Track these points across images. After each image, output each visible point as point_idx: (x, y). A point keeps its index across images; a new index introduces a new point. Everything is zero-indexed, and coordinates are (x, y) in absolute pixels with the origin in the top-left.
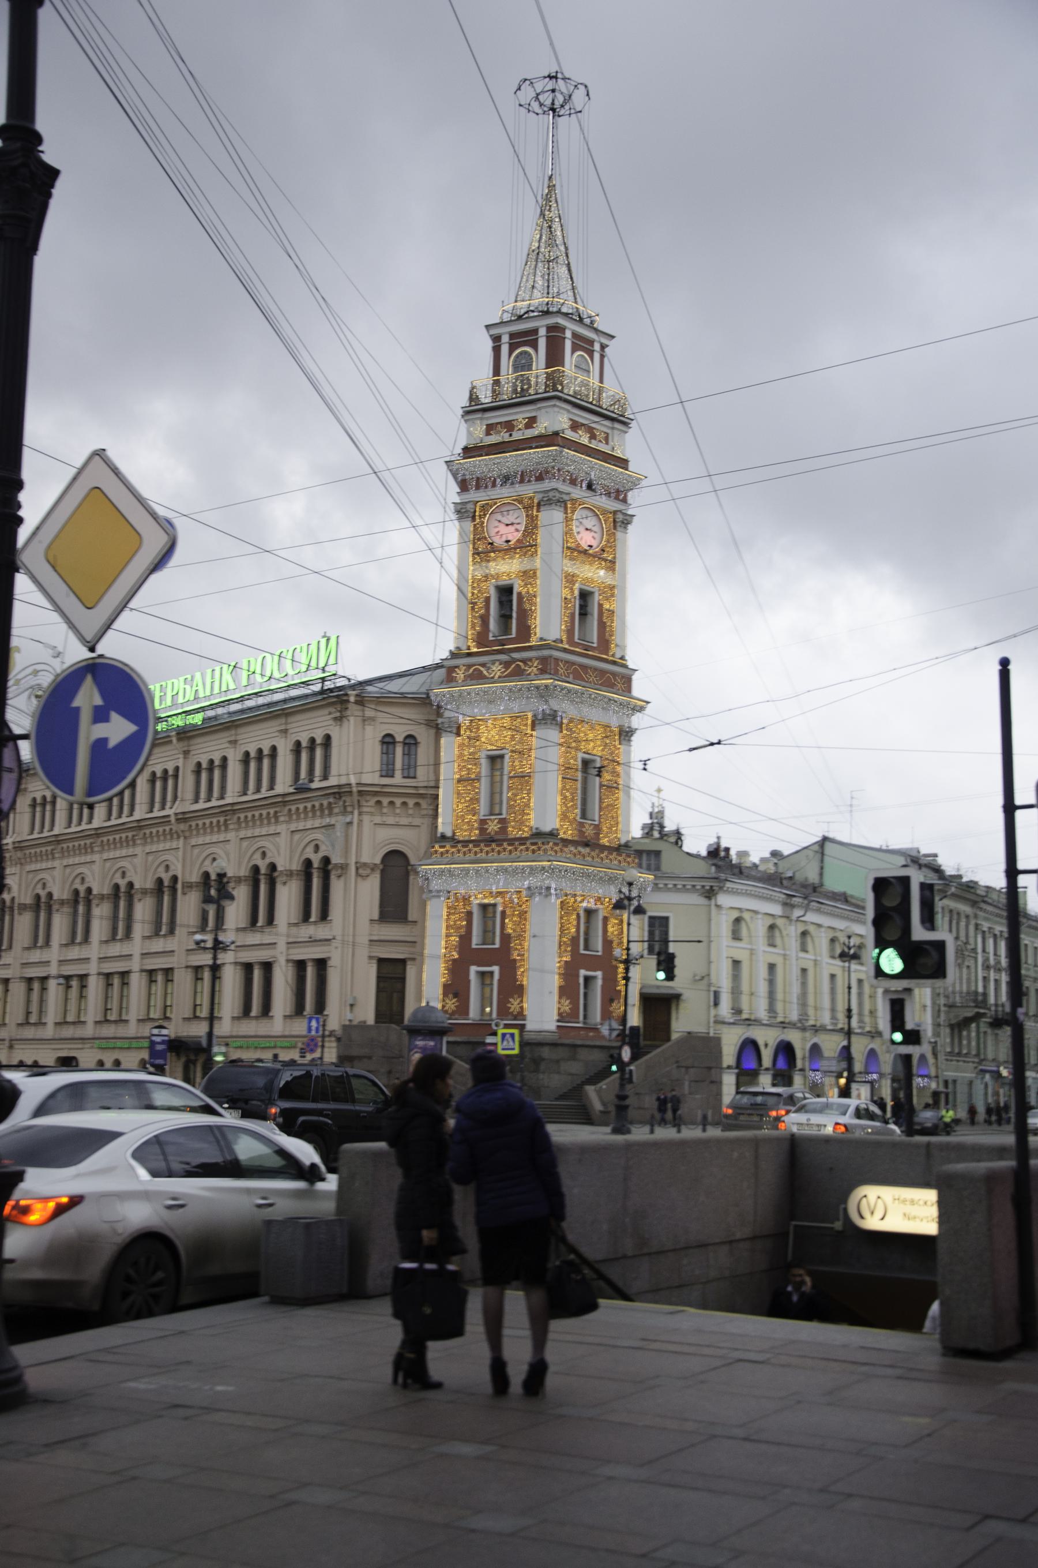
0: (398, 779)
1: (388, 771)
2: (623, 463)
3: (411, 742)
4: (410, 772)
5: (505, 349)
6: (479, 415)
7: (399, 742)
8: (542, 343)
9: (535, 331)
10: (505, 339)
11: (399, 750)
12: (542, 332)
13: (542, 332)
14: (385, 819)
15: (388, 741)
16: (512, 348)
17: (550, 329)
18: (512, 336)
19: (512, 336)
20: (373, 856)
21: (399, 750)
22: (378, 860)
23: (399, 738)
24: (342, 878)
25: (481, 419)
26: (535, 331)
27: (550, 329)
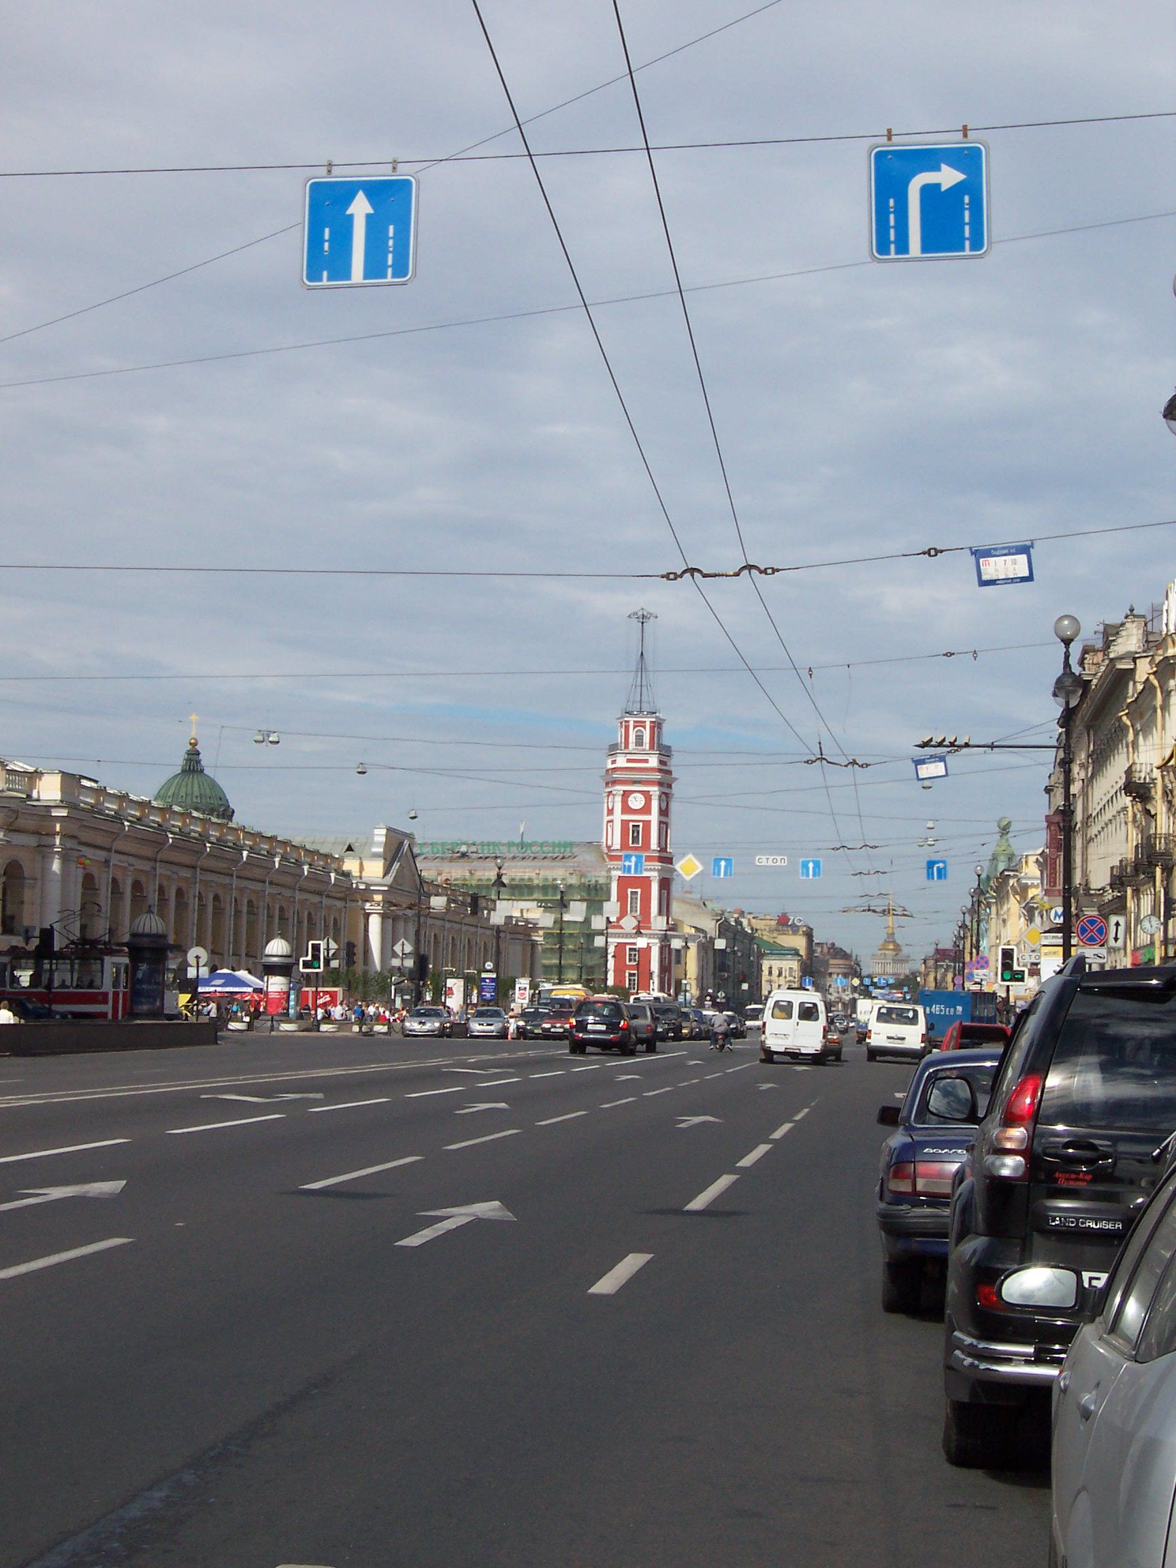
2: (669, 772)
9: (645, 722)
10: (631, 725)
17: (651, 722)
18: (635, 722)
19: (635, 722)
27: (651, 722)
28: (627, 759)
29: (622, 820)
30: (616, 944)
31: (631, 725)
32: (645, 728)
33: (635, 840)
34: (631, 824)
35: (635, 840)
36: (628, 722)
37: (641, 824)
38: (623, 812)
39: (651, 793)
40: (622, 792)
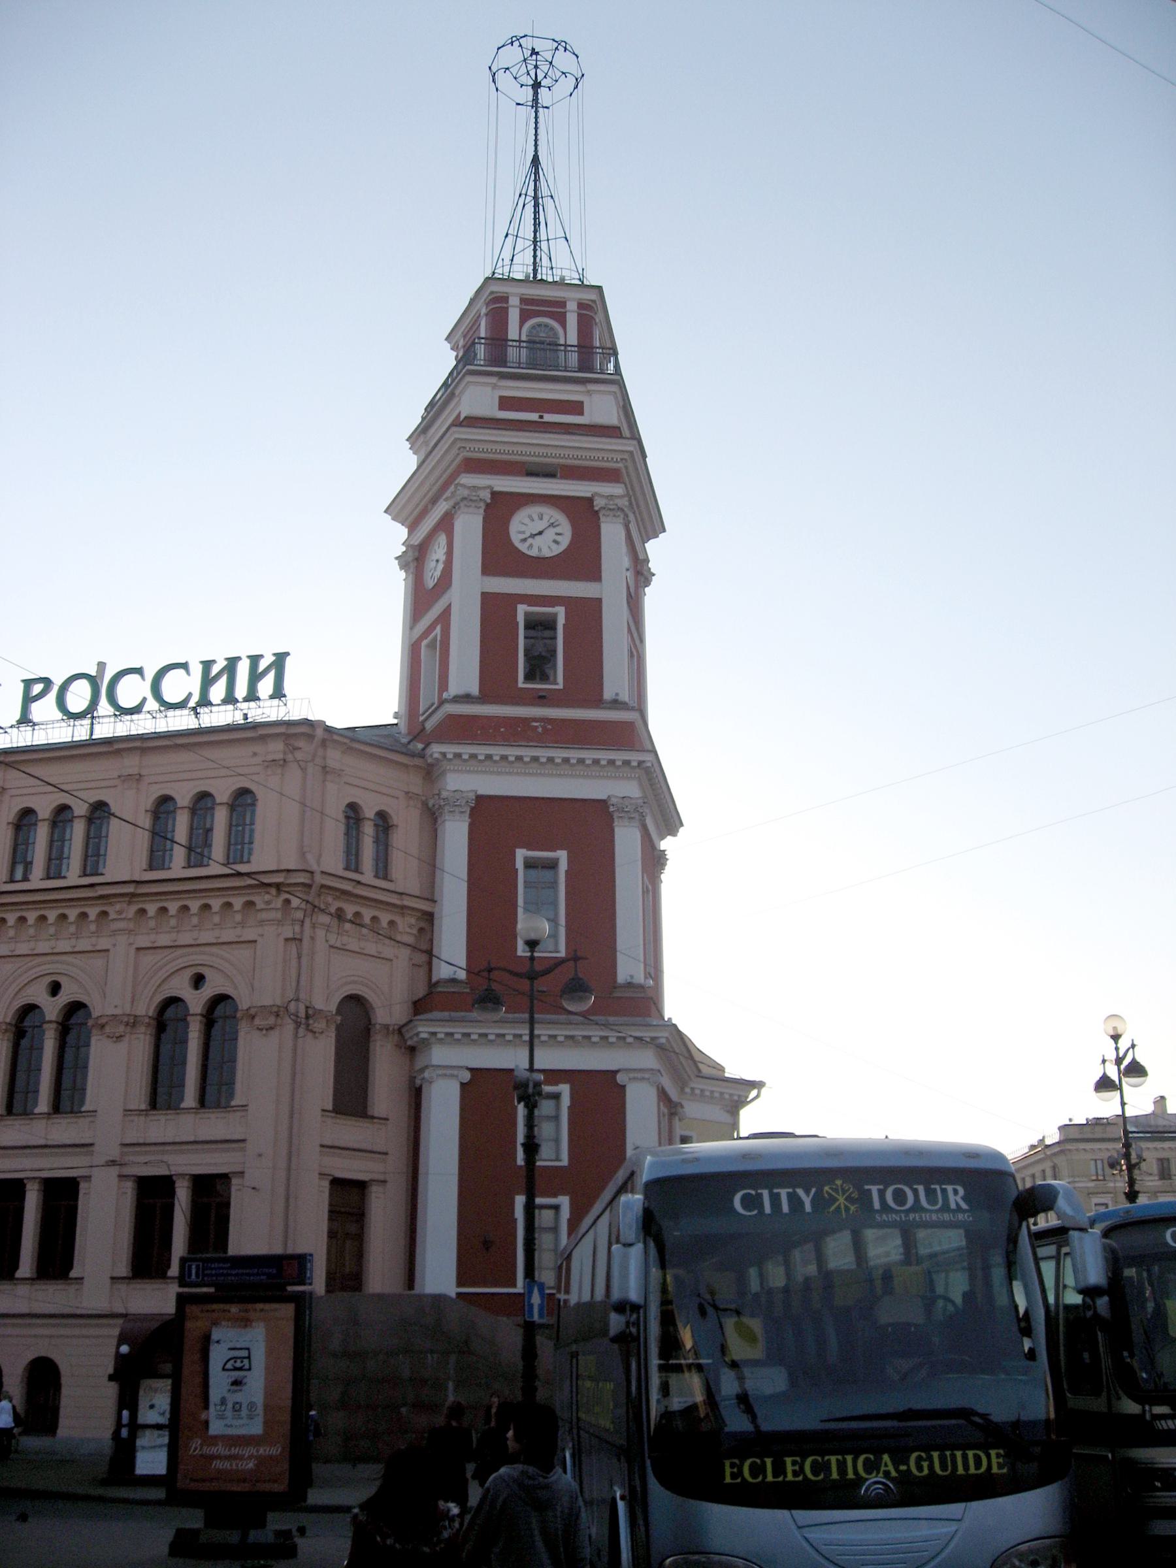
0: (368, 876)
1: (353, 860)
3: (384, 822)
4: (383, 868)
5: (514, 316)
6: (493, 380)
7: (369, 819)
8: (572, 320)
9: (562, 304)
10: (514, 301)
11: (368, 829)
12: (572, 306)
13: (572, 306)
14: (345, 939)
15: (353, 813)
16: (524, 316)
18: (524, 301)
19: (524, 301)
20: (326, 1001)
21: (368, 829)
22: (333, 1008)
23: (369, 812)
24: (274, 1035)
25: (494, 387)
26: (562, 304)
27: (581, 305)
28: (501, 398)
29: (483, 593)
30: (466, 1077)
31: (514, 301)
32: (563, 324)
33: (539, 667)
34: (522, 609)
35: (539, 667)
36: (504, 299)
37: (560, 611)
38: (490, 567)
39: (599, 503)
40: (486, 495)
